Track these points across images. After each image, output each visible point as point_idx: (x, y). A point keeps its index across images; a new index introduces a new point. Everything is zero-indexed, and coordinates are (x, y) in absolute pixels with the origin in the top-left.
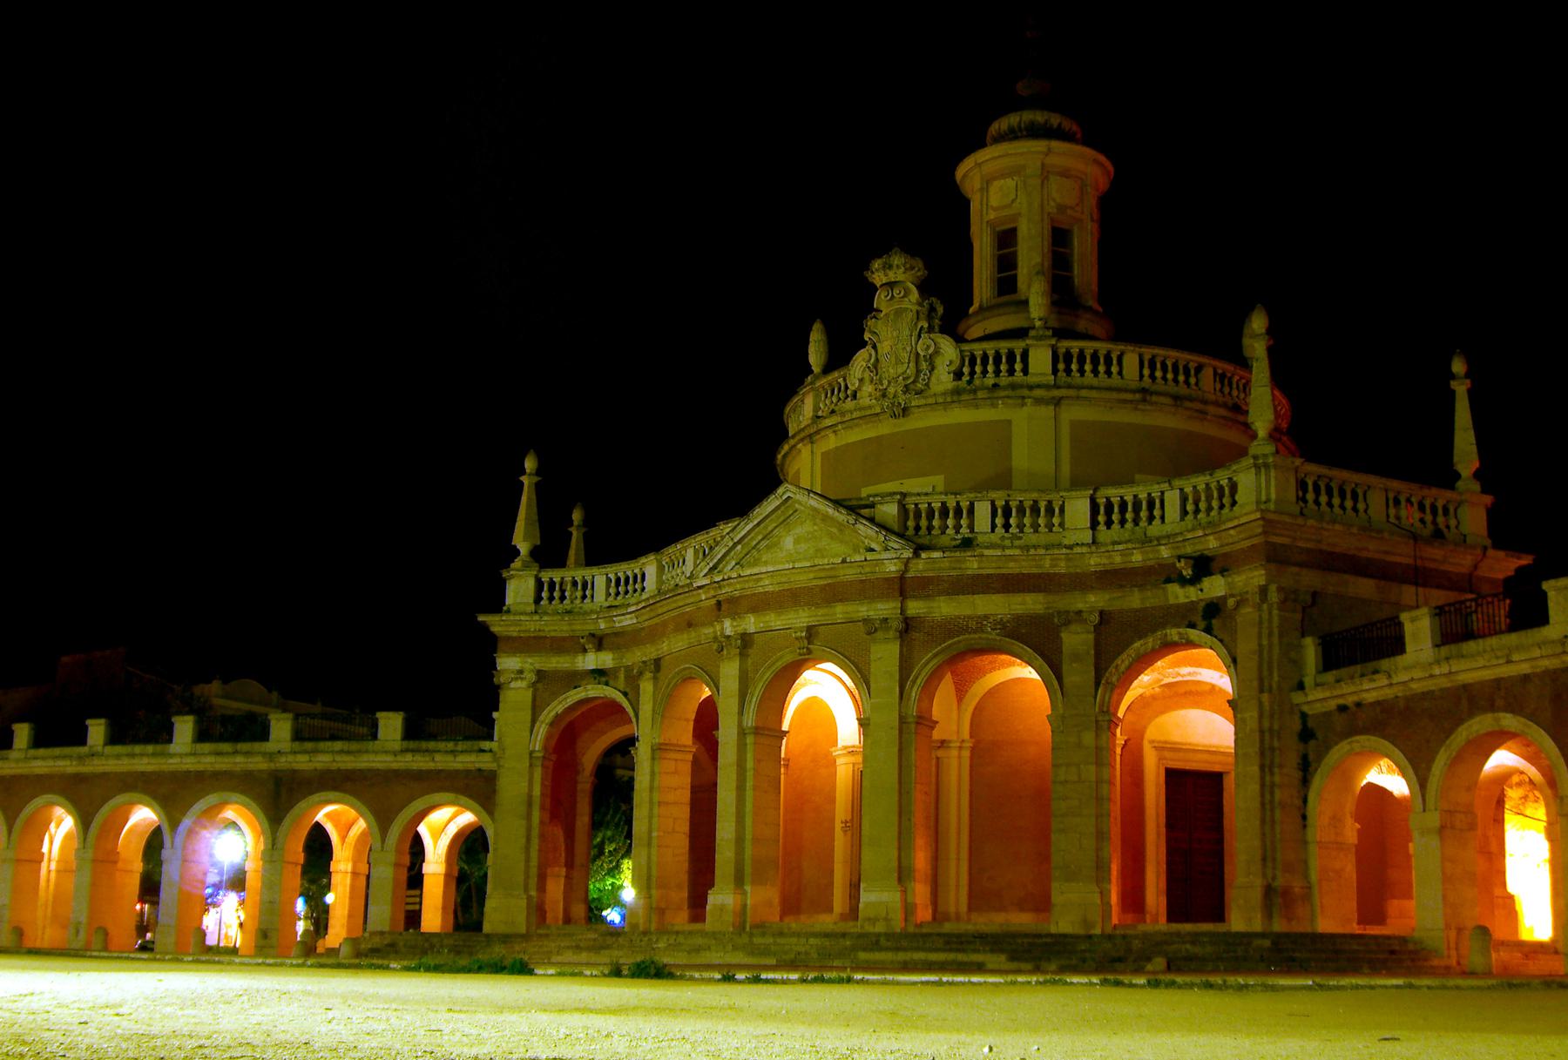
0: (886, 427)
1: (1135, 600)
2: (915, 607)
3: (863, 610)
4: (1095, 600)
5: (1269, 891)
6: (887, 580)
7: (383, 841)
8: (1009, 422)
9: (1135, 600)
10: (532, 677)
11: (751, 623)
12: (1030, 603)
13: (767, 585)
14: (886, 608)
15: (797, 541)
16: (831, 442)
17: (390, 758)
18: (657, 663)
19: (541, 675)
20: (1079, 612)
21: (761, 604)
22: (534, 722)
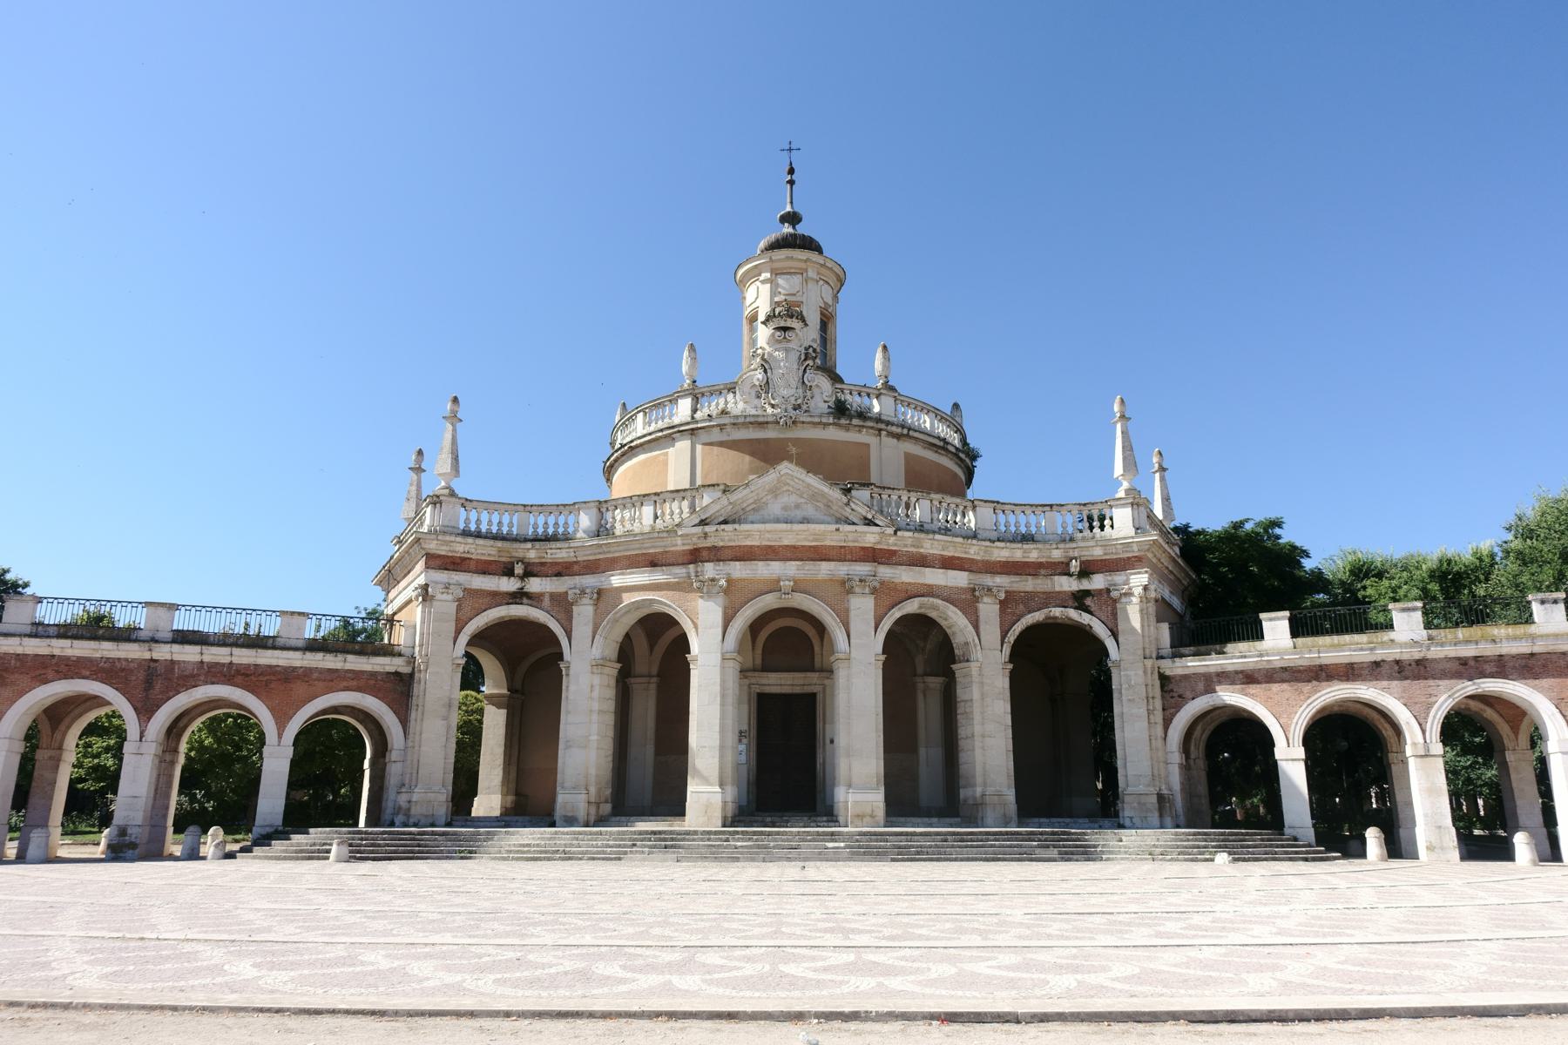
1: (1028, 584)
2: (886, 572)
3: (842, 569)
4: (1001, 581)
5: (1160, 797)
7: (280, 736)
8: (868, 445)
9: (1028, 584)
11: (738, 570)
12: (959, 579)
14: (863, 569)
15: (785, 508)
17: (298, 654)
18: (600, 592)
19: (470, 593)
20: (989, 590)
22: (458, 632)
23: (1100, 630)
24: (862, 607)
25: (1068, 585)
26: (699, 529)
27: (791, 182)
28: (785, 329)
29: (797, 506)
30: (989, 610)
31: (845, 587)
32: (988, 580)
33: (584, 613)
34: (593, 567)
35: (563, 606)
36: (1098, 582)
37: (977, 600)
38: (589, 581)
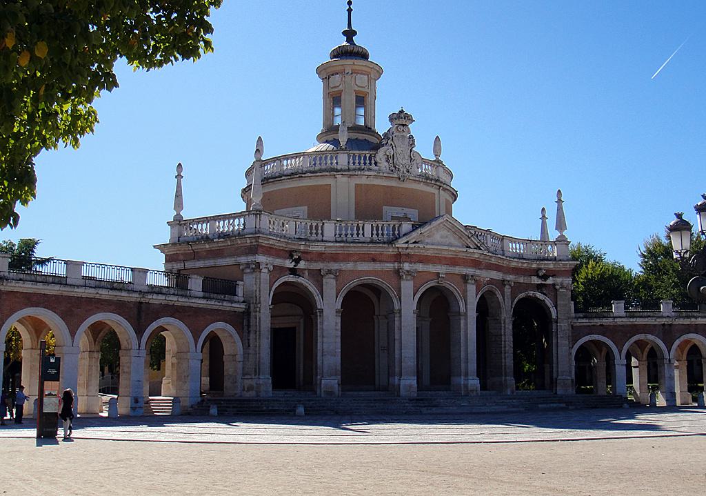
0: (393, 184)
1: (521, 280)
6: (472, 260)
10: (271, 268)
11: (420, 267)
13: (429, 253)
14: (470, 271)
15: (442, 237)
16: (363, 181)
21: (424, 260)
23: (549, 302)
24: (471, 288)
25: (536, 280)
26: (406, 245)
27: (350, 11)
28: (403, 125)
29: (447, 237)
30: (507, 290)
31: (465, 278)
32: (510, 277)
33: (330, 283)
34: (334, 258)
35: (317, 276)
36: (550, 281)
37: (504, 285)
38: (334, 266)
